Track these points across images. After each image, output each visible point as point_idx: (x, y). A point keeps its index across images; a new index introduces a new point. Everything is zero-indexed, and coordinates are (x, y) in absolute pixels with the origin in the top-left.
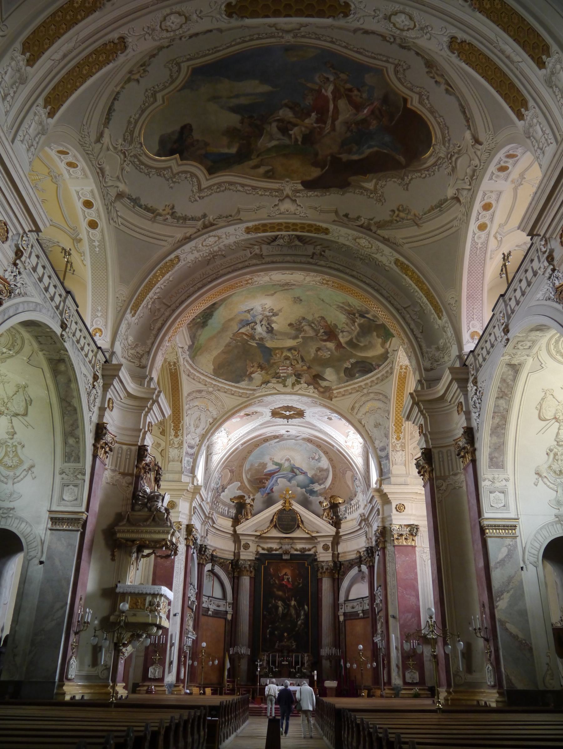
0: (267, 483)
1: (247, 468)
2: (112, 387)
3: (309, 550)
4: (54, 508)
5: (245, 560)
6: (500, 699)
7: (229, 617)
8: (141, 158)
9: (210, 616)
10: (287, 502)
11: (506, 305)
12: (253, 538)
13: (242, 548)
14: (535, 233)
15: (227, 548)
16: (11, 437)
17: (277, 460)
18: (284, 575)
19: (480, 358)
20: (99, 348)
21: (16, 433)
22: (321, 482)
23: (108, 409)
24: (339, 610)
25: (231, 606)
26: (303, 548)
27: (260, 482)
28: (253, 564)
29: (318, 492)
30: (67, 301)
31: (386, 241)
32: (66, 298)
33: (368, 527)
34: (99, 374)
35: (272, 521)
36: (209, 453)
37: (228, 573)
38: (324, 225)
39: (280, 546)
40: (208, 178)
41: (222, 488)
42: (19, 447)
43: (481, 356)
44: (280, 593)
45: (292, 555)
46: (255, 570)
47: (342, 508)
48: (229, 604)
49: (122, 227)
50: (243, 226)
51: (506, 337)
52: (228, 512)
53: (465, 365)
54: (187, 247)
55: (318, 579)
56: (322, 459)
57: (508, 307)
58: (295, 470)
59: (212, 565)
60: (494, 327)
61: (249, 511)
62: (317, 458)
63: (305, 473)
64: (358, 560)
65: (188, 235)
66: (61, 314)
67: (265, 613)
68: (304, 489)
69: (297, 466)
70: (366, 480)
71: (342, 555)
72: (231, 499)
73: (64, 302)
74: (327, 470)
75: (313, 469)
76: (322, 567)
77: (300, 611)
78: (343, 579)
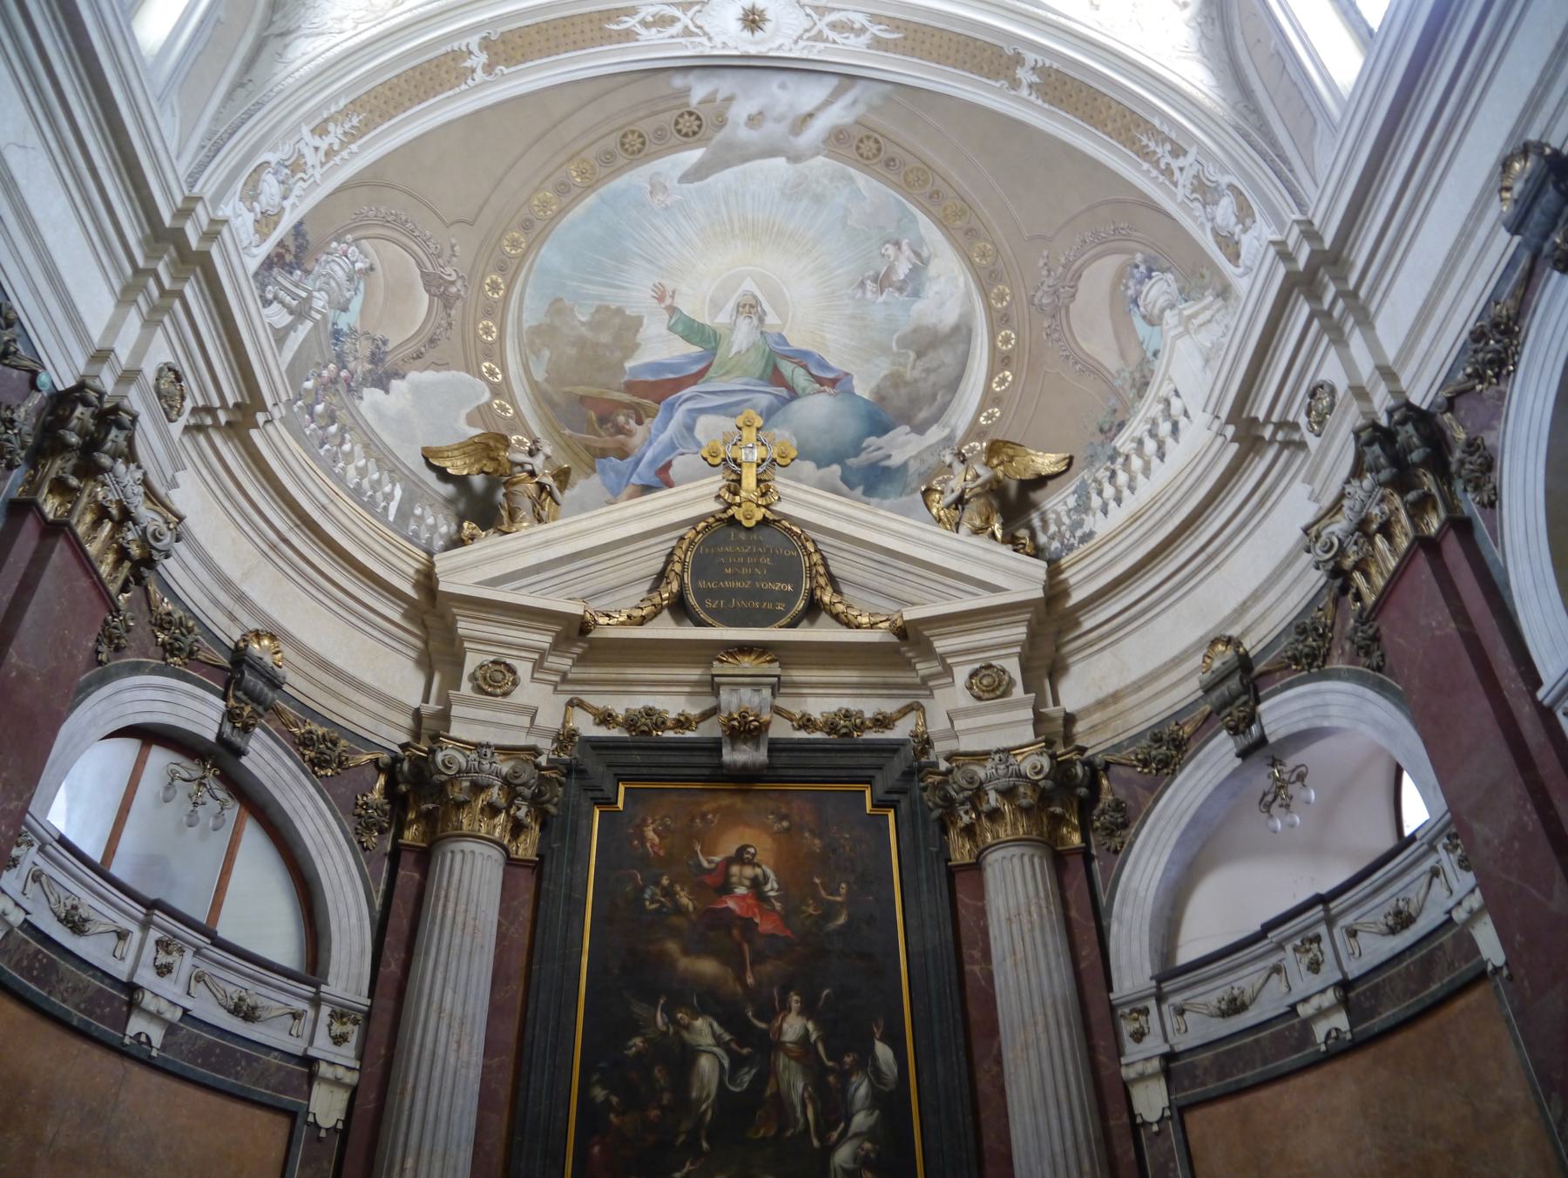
0: (640, 431)
1: (529, 321)
3: (883, 722)
5: (478, 746)
7: (327, 1107)
9: (137, 1055)
10: (749, 480)
12: (544, 640)
13: (466, 687)
15: (368, 678)
17: (693, 306)
18: (729, 862)
22: (923, 415)
24: (1119, 1052)
25: (354, 1033)
26: (847, 715)
27: (603, 420)
28: (527, 774)
29: (913, 467)
33: (1339, 339)
35: (661, 577)
36: (275, 29)
37: (360, 825)
39: (709, 702)
41: (376, 358)
44: (707, 967)
45: (775, 747)
46: (545, 823)
47: (1056, 503)
48: (339, 1015)
52: (404, 514)
55: (952, 873)
56: (932, 270)
58: (787, 368)
59: (230, 715)
61: (526, 504)
62: (902, 270)
63: (835, 382)
64: (1234, 683)
67: (599, 1093)
68: (836, 469)
69: (797, 341)
70: (1255, 136)
71: (1097, 717)
72: (428, 456)
74: (961, 333)
75: (884, 350)
76: (978, 792)
77: (844, 1076)
78: (1119, 852)
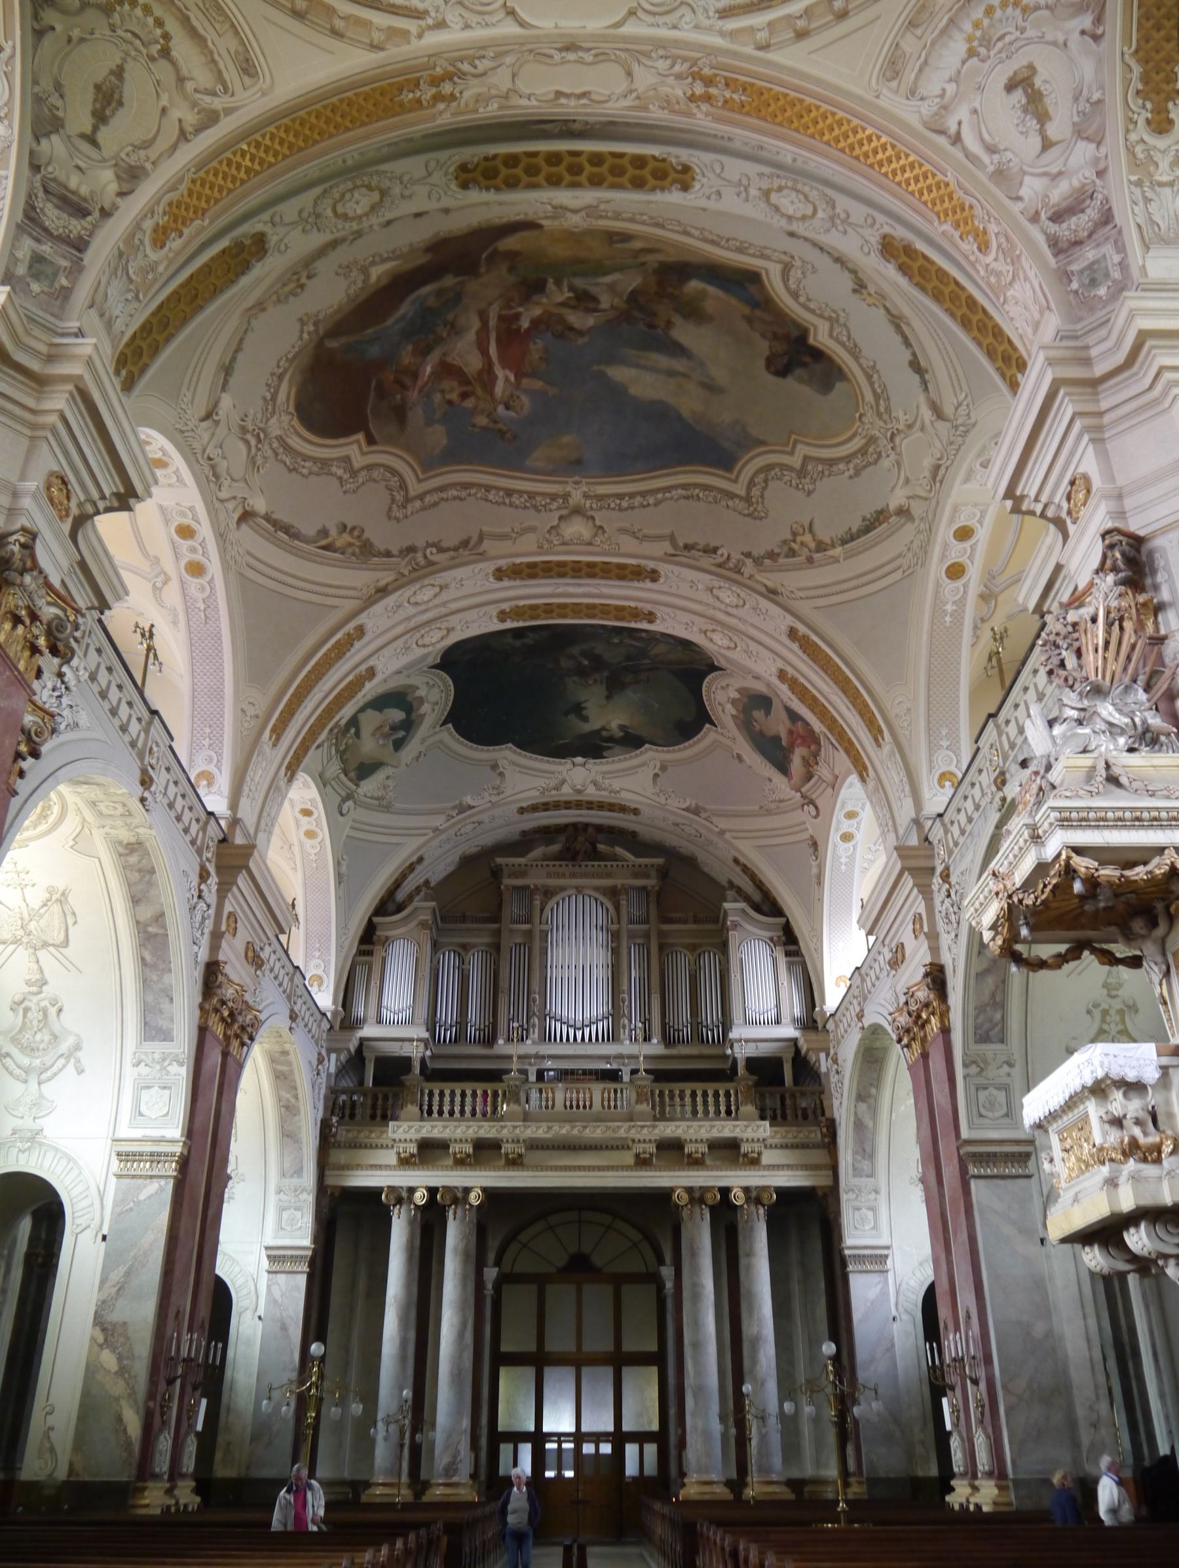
2: (235, 889)
4: (124, 1132)
6: (1001, 1500)
8: (289, 441)
11: (1000, 734)
14: (1045, 609)
16: (34, 989)
19: (955, 830)
20: (211, 814)
21: (45, 983)
23: (227, 935)
30: (152, 730)
31: (772, 594)
32: (150, 723)
34: (211, 868)
38: (651, 565)
40: (421, 476)
42: (53, 1011)
43: (956, 824)
49: (250, 574)
50: (490, 567)
51: (1000, 794)
53: (926, 839)
54: (378, 608)
57: (1004, 738)
60: (980, 771)
65: (382, 583)
66: (141, 756)
73: (147, 731)
